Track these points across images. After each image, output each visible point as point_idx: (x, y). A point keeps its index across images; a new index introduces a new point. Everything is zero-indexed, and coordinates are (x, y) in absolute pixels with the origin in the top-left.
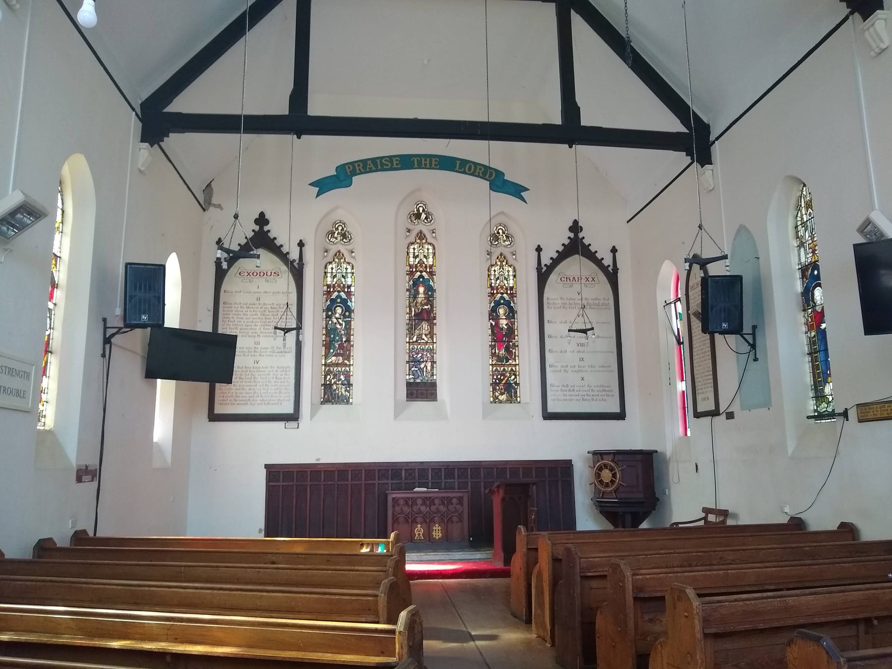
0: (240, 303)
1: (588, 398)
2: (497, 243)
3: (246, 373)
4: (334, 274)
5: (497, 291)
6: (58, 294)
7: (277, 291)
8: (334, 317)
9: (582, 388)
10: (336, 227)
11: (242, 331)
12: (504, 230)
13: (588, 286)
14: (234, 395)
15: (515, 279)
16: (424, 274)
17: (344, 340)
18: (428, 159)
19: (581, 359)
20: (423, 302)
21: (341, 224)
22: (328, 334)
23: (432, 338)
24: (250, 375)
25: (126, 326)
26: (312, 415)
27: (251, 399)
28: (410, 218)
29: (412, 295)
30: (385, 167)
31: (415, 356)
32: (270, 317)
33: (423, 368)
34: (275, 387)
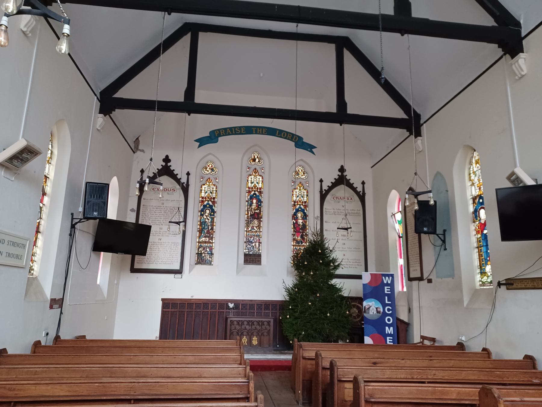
0: (152, 206)
1: (347, 266)
2: (298, 176)
3: (154, 246)
4: (206, 191)
5: (297, 204)
6: (46, 199)
8: (205, 215)
10: (208, 165)
15: (307, 197)
16: (256, 192)
17: (210, 228)
18: (261, 129)
19: (344, 244)
20: (255, 208)
21: (211, 163)
22: (201, 225)
23: (259, 229)
25: (85, 218)
26: (190, 271)
27: (156, 260)
28: (250, 161)
29: (249, 204)
30: (237, 133)
31: (249, 239)
33: (254, 246)
34: (170, 254)
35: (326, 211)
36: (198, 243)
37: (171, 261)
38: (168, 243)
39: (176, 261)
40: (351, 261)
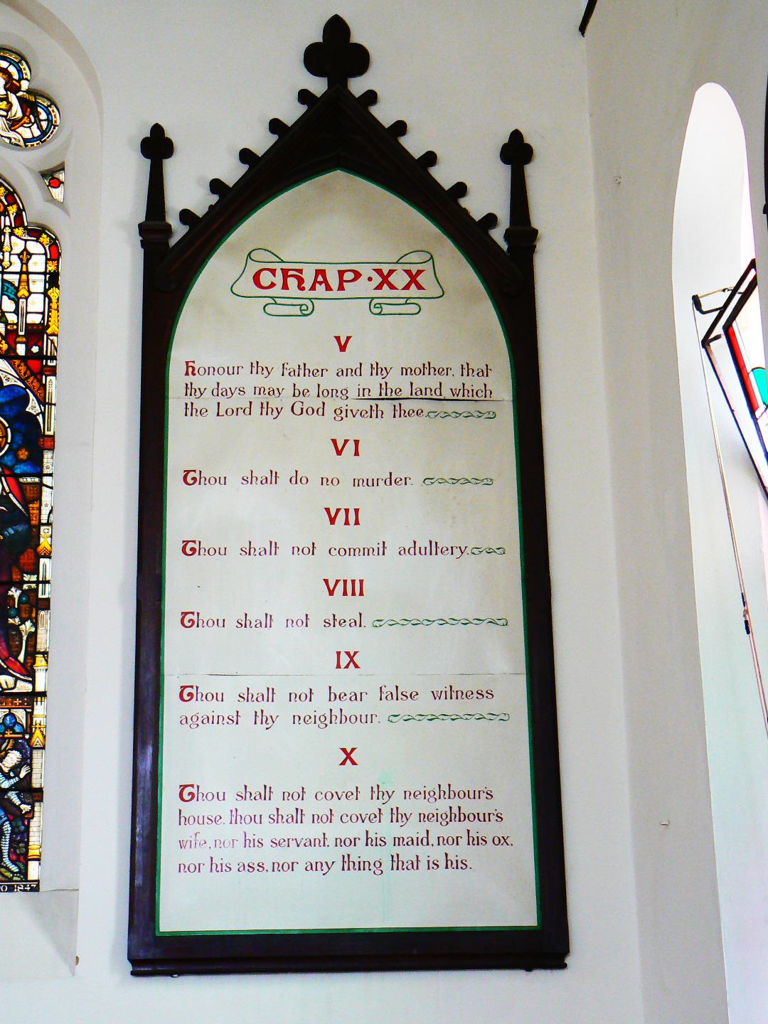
9: (341, 807)
12: (16, 76)
13: (386, 309)
19: (345, 660)
35: (189, 390)
40: (413, 807)
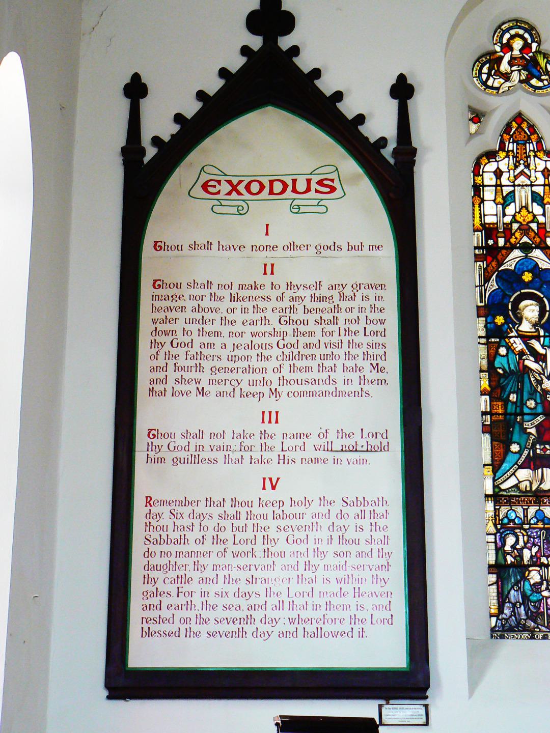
3: (237, 523)
4: (506, 190)
7: (330, 243)
10: (505, 41)
11: (220, 376)
14: (197, 600)
21: (521, 32)
22: (496, 391)
24: (250, 528)
27: (258, 615)
32: (312, 327)
34: (341, 574)
36: (490, 506)
37: (354, 619)
38: (322, 499)
39: (378, 615)
